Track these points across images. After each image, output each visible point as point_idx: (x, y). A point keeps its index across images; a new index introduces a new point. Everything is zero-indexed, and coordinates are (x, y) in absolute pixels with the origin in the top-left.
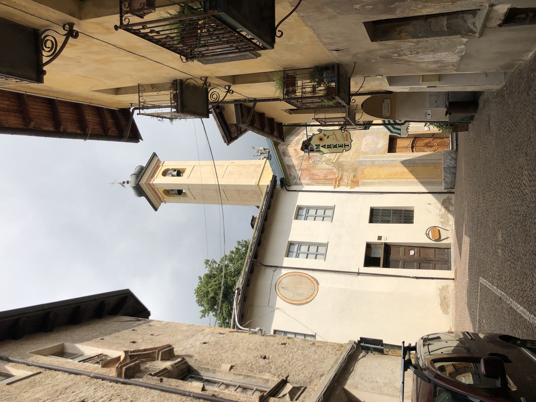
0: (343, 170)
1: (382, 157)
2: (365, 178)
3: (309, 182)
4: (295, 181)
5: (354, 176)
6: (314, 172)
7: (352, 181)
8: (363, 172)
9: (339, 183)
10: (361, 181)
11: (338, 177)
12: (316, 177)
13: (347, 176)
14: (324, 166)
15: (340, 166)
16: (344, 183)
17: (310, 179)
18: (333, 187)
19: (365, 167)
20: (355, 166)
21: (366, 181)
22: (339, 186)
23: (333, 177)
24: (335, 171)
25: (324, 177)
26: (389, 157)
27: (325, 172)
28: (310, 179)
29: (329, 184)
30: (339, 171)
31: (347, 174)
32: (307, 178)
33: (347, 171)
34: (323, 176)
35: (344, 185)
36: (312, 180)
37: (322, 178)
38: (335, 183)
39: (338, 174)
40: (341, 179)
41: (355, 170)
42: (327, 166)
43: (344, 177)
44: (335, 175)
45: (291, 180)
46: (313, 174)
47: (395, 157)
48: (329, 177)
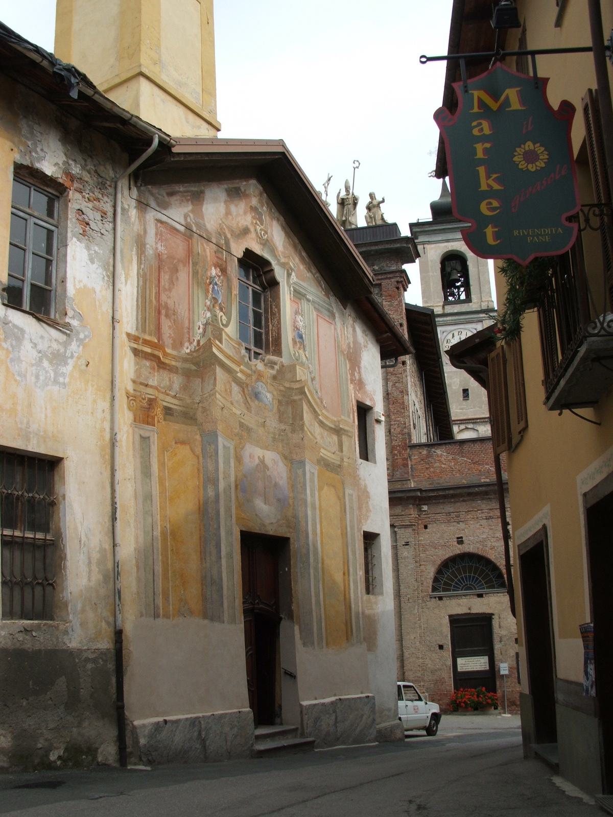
0: (188, 374)
1: (228, 509)
2: (163, 449)
3: (150, 252)
4: (153, 203)
5: (168, 411)
6: (184, 275)
7: (152, 402)
8: (183, 443)
9: (146, 356)
10: (147, 431)
11: (166, 354)
12: (165, 277)
13: (170, 388)
14: (202, 316)
15: (201, 364)
16: (145, 372)
17: (159, 256)
18: (133, 331)
19: (198, 450)
20: (200, 416)
21: (154, 448)
22: (136, 352)
23: (167, 341)
24: (187, 349)
25: (167, 308)
26: (229, 533)
27: (182, 310)
28: (159, 256)
29: (144, 320)
30: (185, 360)
31: (176, 386)
32: (161, 248)
33: (185, 388)
34: (170, 303)
35: (138, 372)
36: (154, 263)
37: (163, 298)
38: (146, 342)
39: (174, 357)
40: (161, 365)
41: (188, 416)
42: (200, 324)
43: (165, 375)
44: (174, 347)
45: (155, 191)
46: (175, 270)
47: (230, 556)
48: (166, 324)
